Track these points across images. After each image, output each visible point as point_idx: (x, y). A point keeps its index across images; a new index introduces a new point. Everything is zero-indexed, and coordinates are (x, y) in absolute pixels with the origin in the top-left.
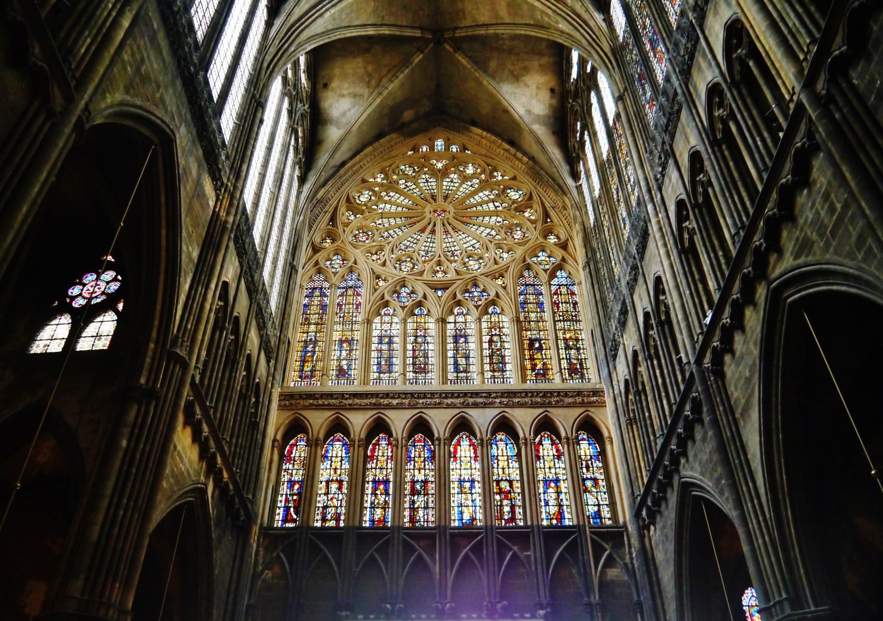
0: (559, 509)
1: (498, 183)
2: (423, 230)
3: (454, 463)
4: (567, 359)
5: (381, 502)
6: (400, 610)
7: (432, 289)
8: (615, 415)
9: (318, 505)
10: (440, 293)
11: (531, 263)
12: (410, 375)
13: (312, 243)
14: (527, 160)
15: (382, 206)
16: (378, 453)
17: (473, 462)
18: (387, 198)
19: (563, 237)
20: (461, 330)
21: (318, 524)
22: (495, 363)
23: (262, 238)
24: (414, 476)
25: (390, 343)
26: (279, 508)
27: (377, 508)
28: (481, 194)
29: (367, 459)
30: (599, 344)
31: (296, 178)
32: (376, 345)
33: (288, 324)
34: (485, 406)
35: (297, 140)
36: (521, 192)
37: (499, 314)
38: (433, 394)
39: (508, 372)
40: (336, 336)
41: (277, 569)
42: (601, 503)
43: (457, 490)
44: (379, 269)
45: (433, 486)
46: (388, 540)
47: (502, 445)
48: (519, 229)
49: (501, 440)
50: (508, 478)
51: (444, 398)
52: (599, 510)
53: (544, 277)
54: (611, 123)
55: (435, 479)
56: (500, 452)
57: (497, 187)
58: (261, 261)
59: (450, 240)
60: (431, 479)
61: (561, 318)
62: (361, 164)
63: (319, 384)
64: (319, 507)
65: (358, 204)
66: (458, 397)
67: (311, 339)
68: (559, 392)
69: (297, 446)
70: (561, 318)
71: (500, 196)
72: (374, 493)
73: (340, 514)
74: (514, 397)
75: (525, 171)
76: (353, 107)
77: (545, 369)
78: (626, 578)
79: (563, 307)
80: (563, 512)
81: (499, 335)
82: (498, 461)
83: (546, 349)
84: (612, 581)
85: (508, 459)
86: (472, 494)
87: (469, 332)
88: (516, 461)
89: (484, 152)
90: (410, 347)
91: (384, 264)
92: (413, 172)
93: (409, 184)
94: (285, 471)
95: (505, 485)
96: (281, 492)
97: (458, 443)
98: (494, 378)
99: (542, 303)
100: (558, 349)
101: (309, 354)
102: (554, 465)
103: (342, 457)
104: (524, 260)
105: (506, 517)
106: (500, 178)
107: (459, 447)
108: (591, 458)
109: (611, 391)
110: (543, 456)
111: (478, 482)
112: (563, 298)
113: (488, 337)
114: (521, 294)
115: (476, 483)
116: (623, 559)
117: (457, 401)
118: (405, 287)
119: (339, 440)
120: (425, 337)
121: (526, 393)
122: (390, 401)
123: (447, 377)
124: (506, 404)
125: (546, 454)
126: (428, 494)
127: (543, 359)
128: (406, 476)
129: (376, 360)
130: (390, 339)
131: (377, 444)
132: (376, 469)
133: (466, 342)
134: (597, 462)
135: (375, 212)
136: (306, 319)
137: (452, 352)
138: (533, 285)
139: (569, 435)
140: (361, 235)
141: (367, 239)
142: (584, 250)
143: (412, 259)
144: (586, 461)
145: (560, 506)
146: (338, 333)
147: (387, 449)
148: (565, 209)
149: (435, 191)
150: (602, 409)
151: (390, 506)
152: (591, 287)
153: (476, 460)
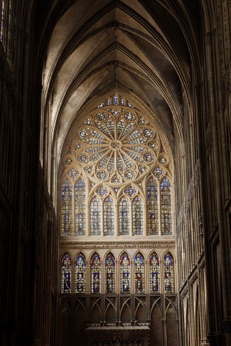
2: (109, 155)
6: (105, 323)
18: (93, 134)
19: (168, 160)
25: (98, 215)
28: (134, 133)
34: (133, 247)
38: (114, 243)
40: (77, 212)
41: (65, 309)
44: (92, 179)
46: (100, 299)
47: (138, 259)
53: (158, 183)
76: (78, 96)
84: (171, 313)
90: (105, 217)
92: (104, 118)
94: (63, 269)
97: (123, 259)
99: (157, 196)
112: (165, 193)
121: (147, 242)
130: (97, 214)
131: (95, 258)
133: (127, 215)
145: (157, 283)
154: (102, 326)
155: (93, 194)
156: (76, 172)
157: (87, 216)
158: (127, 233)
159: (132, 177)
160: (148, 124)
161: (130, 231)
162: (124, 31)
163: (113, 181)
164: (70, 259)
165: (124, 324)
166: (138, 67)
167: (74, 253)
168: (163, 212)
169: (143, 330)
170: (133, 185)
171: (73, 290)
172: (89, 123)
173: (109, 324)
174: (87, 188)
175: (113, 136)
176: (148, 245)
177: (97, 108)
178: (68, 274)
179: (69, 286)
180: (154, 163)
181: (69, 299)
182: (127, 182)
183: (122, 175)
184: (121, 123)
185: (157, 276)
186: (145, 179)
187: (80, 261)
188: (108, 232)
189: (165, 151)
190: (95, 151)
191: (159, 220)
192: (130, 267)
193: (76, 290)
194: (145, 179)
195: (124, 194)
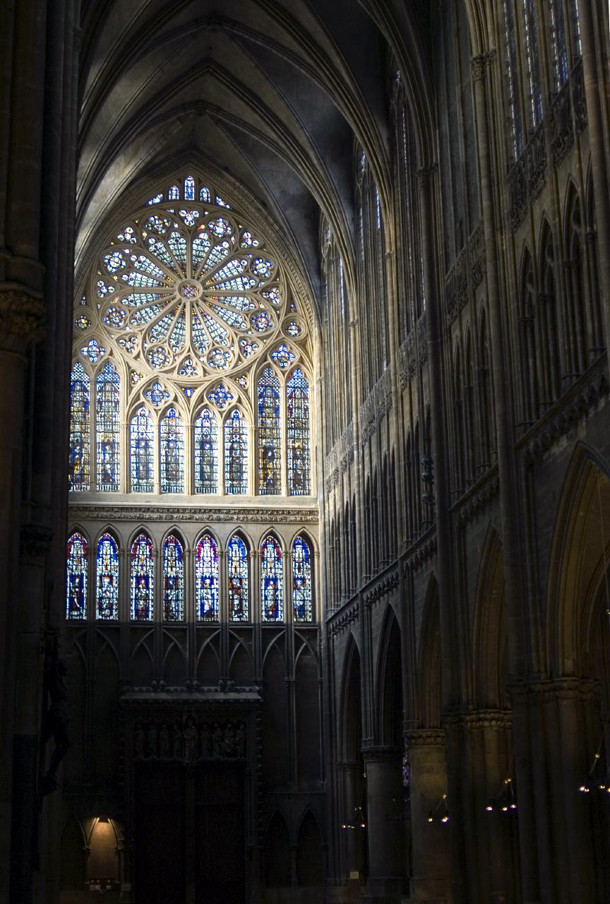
4: (293, 469)
11: (272, 363)
12: (164, 482)
14: (278, 228)
15: (132, 275)
17: (213, 562)
20: (206, 436)
25: (147, 447)
28: (230, 265)
34: (227, 521)
36: (268, 264)
38: (184, 510)
42: (306, 598)
43: (199, 586)
44: (134, 364)
46: (152, 634)
47: (235, 547)
49: (235, 543)
52: (304, 604)
53: (281, 379)
56: (234, 553)
60: (180, 576)
61: (293, 425)
67: (78, 440)
68: (283, 511)
69: (74, 544)
70: (293, 425)
72: (137, 587)
73: (112, 604)
78: (315, 663)
79: (296, 413)
80: (278, 605)
82: (232, 561)
86: (211, 589)
87: (213, 437)
92: (163, 228)
93: (159, 245)
95: (236, 583)
98: (233, 487)
103: (110, 555)
105: (236, 609)
107: (202, 549)
108: (303, 561)
112: (297, 403)
113: (230, 444)
114: (261, 396)
116: (314, 649)
118: (158, 384)
119: (107, 540)
120: (176, 441)
121: (258, 511)
122: (152, 515)
123: (194, 484)
126: (178, 589)
127: (274, 469)
129: (135, 465)
130: (146, 444)
132: (138, 566)
133: (211, 449)
138: (271, 387)
142: (319, 365)
143: (163, 349)
144: (299, 563)
145: (276, 600)
149: (185, 257)
150: (315, 526)
154: (155, 691)
155: (138, 398)
157: (121, 450)
158: (211, 488)
159: (225, 365)
160: (261, 247)
161: (219, 484)
162: (233, 37)
163: (183, 369)
164: (84, 544)
165: (206, 688)
166: (252, 118)
167: (95, 528)
168: (290, 444)
169: (247, 701)
170: (228, 383)
171: (91, 613)
172: (128, 237)
173: (172, 688)
174: (122, 386)
175: (184, 270)
176: (259, 517)
177: (146, 205)
178: (78, 576)
179: (81, 602)
180: (274, 336)
181: (85, 630)
182: (214, 376)
183: (202, 359)
184: (202, 243)
185: (275, 584)
187: (107, 549)
188: (169, 485)
189: (298, 309)
190: (141, 303)
191: (283, 461)
193: (97, 611)
195: (206, 401)
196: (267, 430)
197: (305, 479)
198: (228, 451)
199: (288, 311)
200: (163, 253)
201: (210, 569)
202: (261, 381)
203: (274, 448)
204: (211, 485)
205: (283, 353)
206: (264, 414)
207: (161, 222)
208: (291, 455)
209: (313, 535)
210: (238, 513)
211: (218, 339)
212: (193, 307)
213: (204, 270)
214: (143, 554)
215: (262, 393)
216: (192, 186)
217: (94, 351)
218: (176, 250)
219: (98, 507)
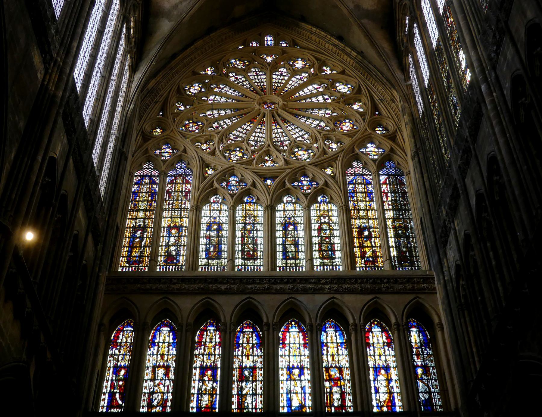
0: (390, 397)
1: (327, 77)
3: (283, 350)
5: (208, 388)
7: (261, 178)
8: (446, 302)
9: (144, 391)
10: (269, 182)
11: (360, 153)
13: (142, 132)
14: (356, 54)
15: (212, 97)
16: (206, 339)
17: (302, 348)
18: (216, 90)
19: (391, 128)
20: (290, 218)
21: (144, 410)
22: (324, 250)
23: (91, 120)
24: (242, 362)
25: (219, 229)
26: (105, 394)
27: (205, 394)
28: (310, 87)
29: (194, 345)
30: (429, 232)
31: (127, 67)
32: (205, 232)
33: (116, 209)
34: (314, 292)
35: (128, 29)
36: (349, 86)
37: (328, 203)
39: (337, 260)
42: (433, 390)
43: (285, 379)
44: (209, 159)
45: (261, 372)
47: (331, 331)
48: (347, 121)
49: (330, 327)
50: (337, 365)
51: (273, 284)
52: (430, 397)
54: (441, 11)
55: (264, 365)
56: (329, 339)
57: (326, 81)
58: (90, 142)
59: (279, 130)
62: (192, 56)
63: (146, 270)
64: (145, 393)
65: (188, 95)
66: (287, 283)
67: (140, 225)
68: (389, 279)
69: (123, 331)
71: (329, 90)
72: (201, 380)
73: (166, 400)
74: (344, 283)
75: (354, 65)
77: (375, 257)
81: (329, 223)
82: (328, 347)
83: (376, 237)
85: (337, 346)
86: (301, 381)
87: (298, 219)
88: (346, 349)
89: (313, 47)
90: (238, 234)
91: (213, 153)
93: (239, 77)
94: (111, 356)
95: (334, 373)
96: (107, 378)
97: (287, 330)
99: (371, 193)
100: (387, 237)
101: (137, 240)
102: (384, 353)
104: (353, 151)
105: (336, 404)
106: (329, 72)
107: (288, 334)
109: (441, 277)
110: (373, 344)
111: (307, 368)
114: (350, 183)
115: (306, 369)
117: (287, 287)
119: (167, 326)
120: (254, 224)
122: (219, 286)
124: (336, 290)
125: (376, 341)
128: (233, 363)
129: (204, 247)
132: (203, 355)
133: (295, 229)
134: (428, 349)
135: (204, 103)
136: (135, 205)
137: (281, 239)
138: (362, 175)
139: (400, 322)
140: (191, 125)
141: (197, 129)
142: (413, 140)
143: (241, 148)
145: (391, 393)
146: (167, 220)
147: (215, 335)
148: (394, 102)
151: (218, 392)
152: (420, 176)
153: (304, 347)
156: (172, 149)
186: (340, 159)
189: (384, 112)
192: (307, 353)
194: (340, 159)
196: (360, 211)
197: (411, 255)
198: (316, 232)
199: (373, 114)
200: (243, 81)
201: (298, 358)
202: (350, 171)
203: (372, 228)
204: (296, 265)
205: (372, 149)
206: (355, 198)
207: (241, 62)
208: (392, 233)
209: (431, 306)
210: (331, 283)
211: (300, 139)
212: (273, 116)
213: (284, 92)
214: (211, 342)
215: (352, 181)
216: (271, 40)
217: (168, 152)
218: (256, 79)
219: (153, 279)
